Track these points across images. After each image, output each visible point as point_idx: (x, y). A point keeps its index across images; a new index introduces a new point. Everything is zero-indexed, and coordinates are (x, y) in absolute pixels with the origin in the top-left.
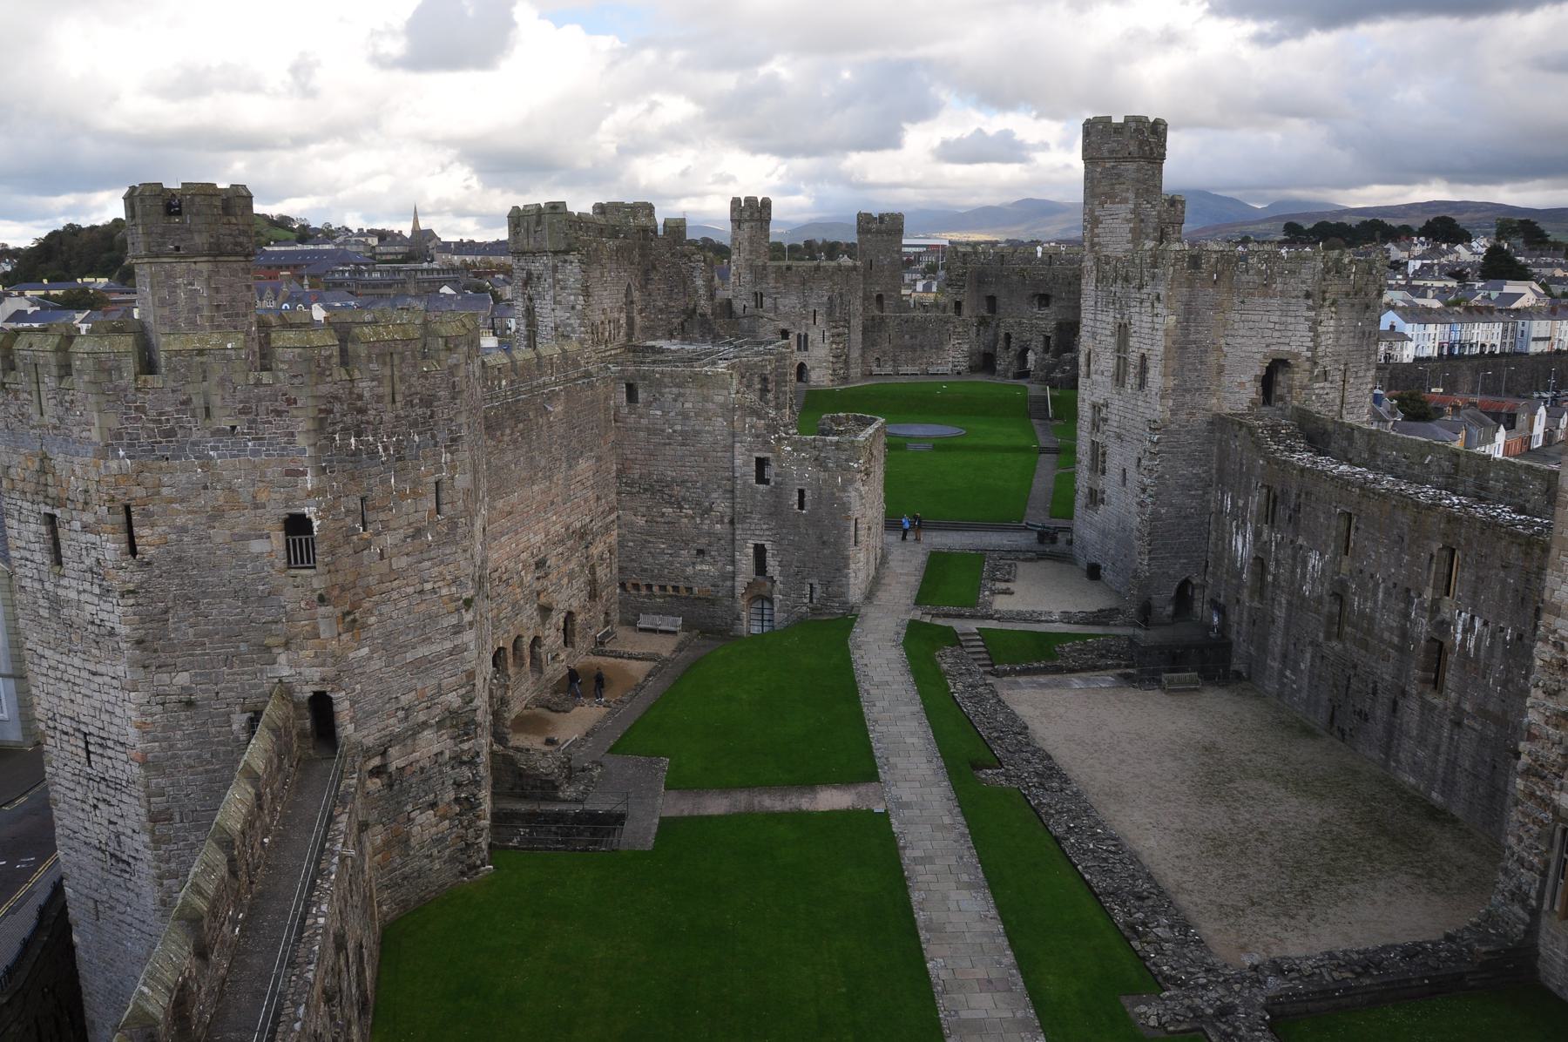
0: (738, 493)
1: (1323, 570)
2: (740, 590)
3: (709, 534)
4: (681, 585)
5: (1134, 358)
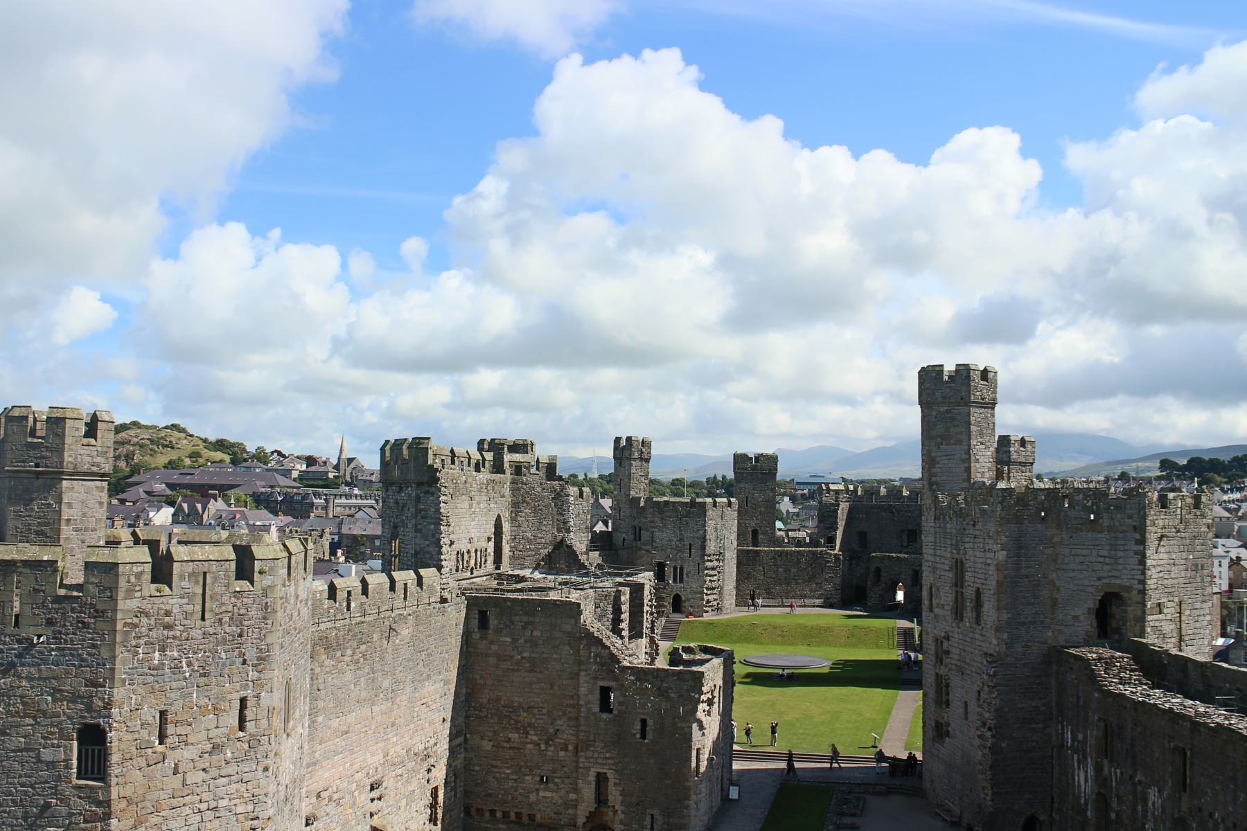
1: (1163, 808)
2: (581, 820)
3: (553, 760)
4: (525, 811)
5: (969, 592)
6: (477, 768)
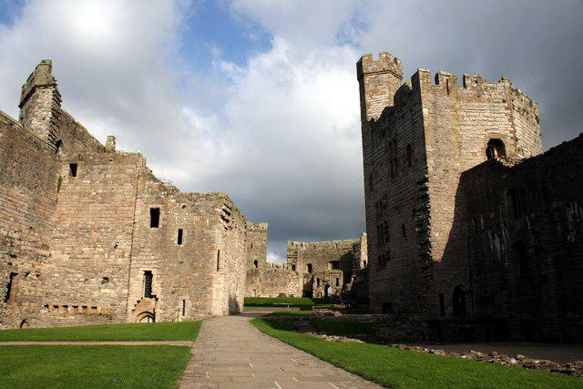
0: (135, 234)
2: (131, 307)
3: (113, 266)
4: (89, 305)
6: (57, 275)
